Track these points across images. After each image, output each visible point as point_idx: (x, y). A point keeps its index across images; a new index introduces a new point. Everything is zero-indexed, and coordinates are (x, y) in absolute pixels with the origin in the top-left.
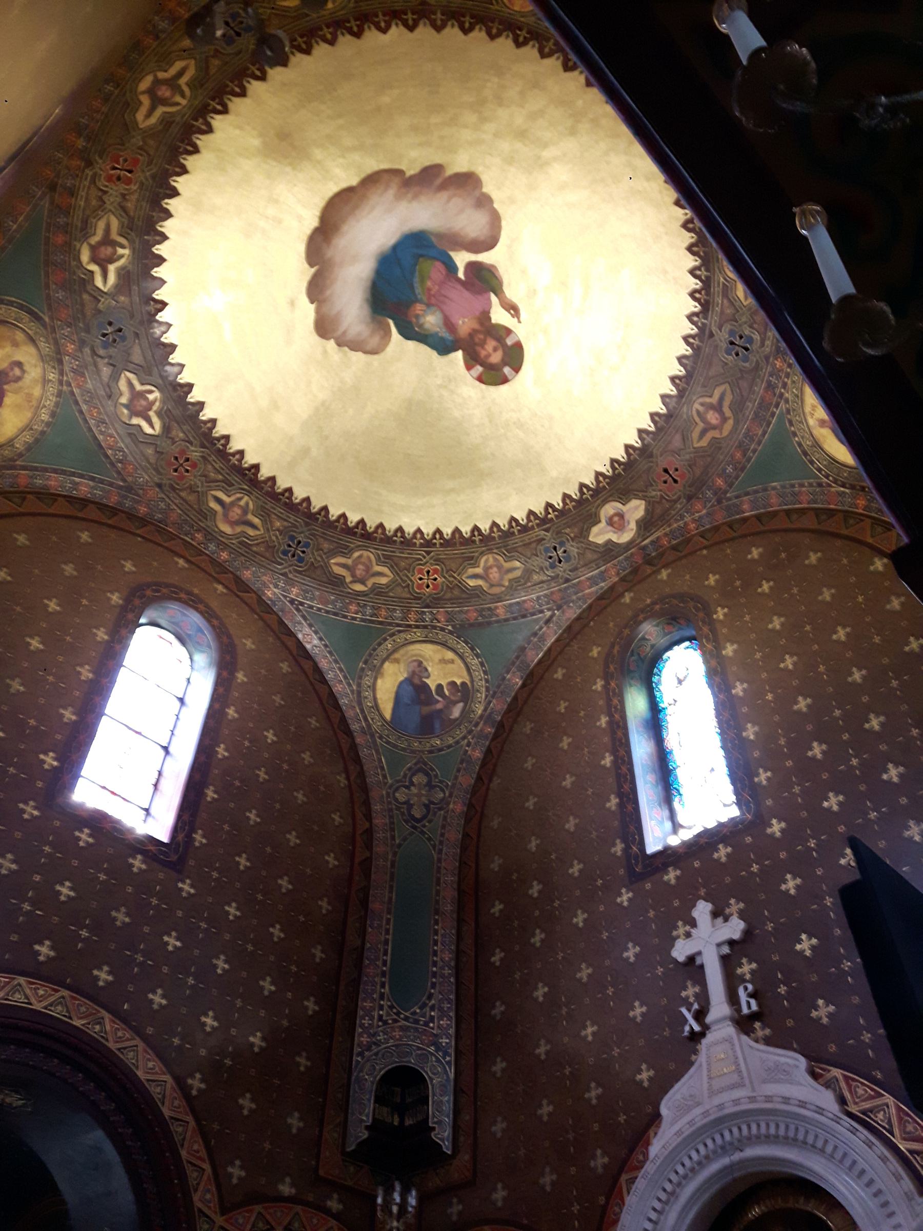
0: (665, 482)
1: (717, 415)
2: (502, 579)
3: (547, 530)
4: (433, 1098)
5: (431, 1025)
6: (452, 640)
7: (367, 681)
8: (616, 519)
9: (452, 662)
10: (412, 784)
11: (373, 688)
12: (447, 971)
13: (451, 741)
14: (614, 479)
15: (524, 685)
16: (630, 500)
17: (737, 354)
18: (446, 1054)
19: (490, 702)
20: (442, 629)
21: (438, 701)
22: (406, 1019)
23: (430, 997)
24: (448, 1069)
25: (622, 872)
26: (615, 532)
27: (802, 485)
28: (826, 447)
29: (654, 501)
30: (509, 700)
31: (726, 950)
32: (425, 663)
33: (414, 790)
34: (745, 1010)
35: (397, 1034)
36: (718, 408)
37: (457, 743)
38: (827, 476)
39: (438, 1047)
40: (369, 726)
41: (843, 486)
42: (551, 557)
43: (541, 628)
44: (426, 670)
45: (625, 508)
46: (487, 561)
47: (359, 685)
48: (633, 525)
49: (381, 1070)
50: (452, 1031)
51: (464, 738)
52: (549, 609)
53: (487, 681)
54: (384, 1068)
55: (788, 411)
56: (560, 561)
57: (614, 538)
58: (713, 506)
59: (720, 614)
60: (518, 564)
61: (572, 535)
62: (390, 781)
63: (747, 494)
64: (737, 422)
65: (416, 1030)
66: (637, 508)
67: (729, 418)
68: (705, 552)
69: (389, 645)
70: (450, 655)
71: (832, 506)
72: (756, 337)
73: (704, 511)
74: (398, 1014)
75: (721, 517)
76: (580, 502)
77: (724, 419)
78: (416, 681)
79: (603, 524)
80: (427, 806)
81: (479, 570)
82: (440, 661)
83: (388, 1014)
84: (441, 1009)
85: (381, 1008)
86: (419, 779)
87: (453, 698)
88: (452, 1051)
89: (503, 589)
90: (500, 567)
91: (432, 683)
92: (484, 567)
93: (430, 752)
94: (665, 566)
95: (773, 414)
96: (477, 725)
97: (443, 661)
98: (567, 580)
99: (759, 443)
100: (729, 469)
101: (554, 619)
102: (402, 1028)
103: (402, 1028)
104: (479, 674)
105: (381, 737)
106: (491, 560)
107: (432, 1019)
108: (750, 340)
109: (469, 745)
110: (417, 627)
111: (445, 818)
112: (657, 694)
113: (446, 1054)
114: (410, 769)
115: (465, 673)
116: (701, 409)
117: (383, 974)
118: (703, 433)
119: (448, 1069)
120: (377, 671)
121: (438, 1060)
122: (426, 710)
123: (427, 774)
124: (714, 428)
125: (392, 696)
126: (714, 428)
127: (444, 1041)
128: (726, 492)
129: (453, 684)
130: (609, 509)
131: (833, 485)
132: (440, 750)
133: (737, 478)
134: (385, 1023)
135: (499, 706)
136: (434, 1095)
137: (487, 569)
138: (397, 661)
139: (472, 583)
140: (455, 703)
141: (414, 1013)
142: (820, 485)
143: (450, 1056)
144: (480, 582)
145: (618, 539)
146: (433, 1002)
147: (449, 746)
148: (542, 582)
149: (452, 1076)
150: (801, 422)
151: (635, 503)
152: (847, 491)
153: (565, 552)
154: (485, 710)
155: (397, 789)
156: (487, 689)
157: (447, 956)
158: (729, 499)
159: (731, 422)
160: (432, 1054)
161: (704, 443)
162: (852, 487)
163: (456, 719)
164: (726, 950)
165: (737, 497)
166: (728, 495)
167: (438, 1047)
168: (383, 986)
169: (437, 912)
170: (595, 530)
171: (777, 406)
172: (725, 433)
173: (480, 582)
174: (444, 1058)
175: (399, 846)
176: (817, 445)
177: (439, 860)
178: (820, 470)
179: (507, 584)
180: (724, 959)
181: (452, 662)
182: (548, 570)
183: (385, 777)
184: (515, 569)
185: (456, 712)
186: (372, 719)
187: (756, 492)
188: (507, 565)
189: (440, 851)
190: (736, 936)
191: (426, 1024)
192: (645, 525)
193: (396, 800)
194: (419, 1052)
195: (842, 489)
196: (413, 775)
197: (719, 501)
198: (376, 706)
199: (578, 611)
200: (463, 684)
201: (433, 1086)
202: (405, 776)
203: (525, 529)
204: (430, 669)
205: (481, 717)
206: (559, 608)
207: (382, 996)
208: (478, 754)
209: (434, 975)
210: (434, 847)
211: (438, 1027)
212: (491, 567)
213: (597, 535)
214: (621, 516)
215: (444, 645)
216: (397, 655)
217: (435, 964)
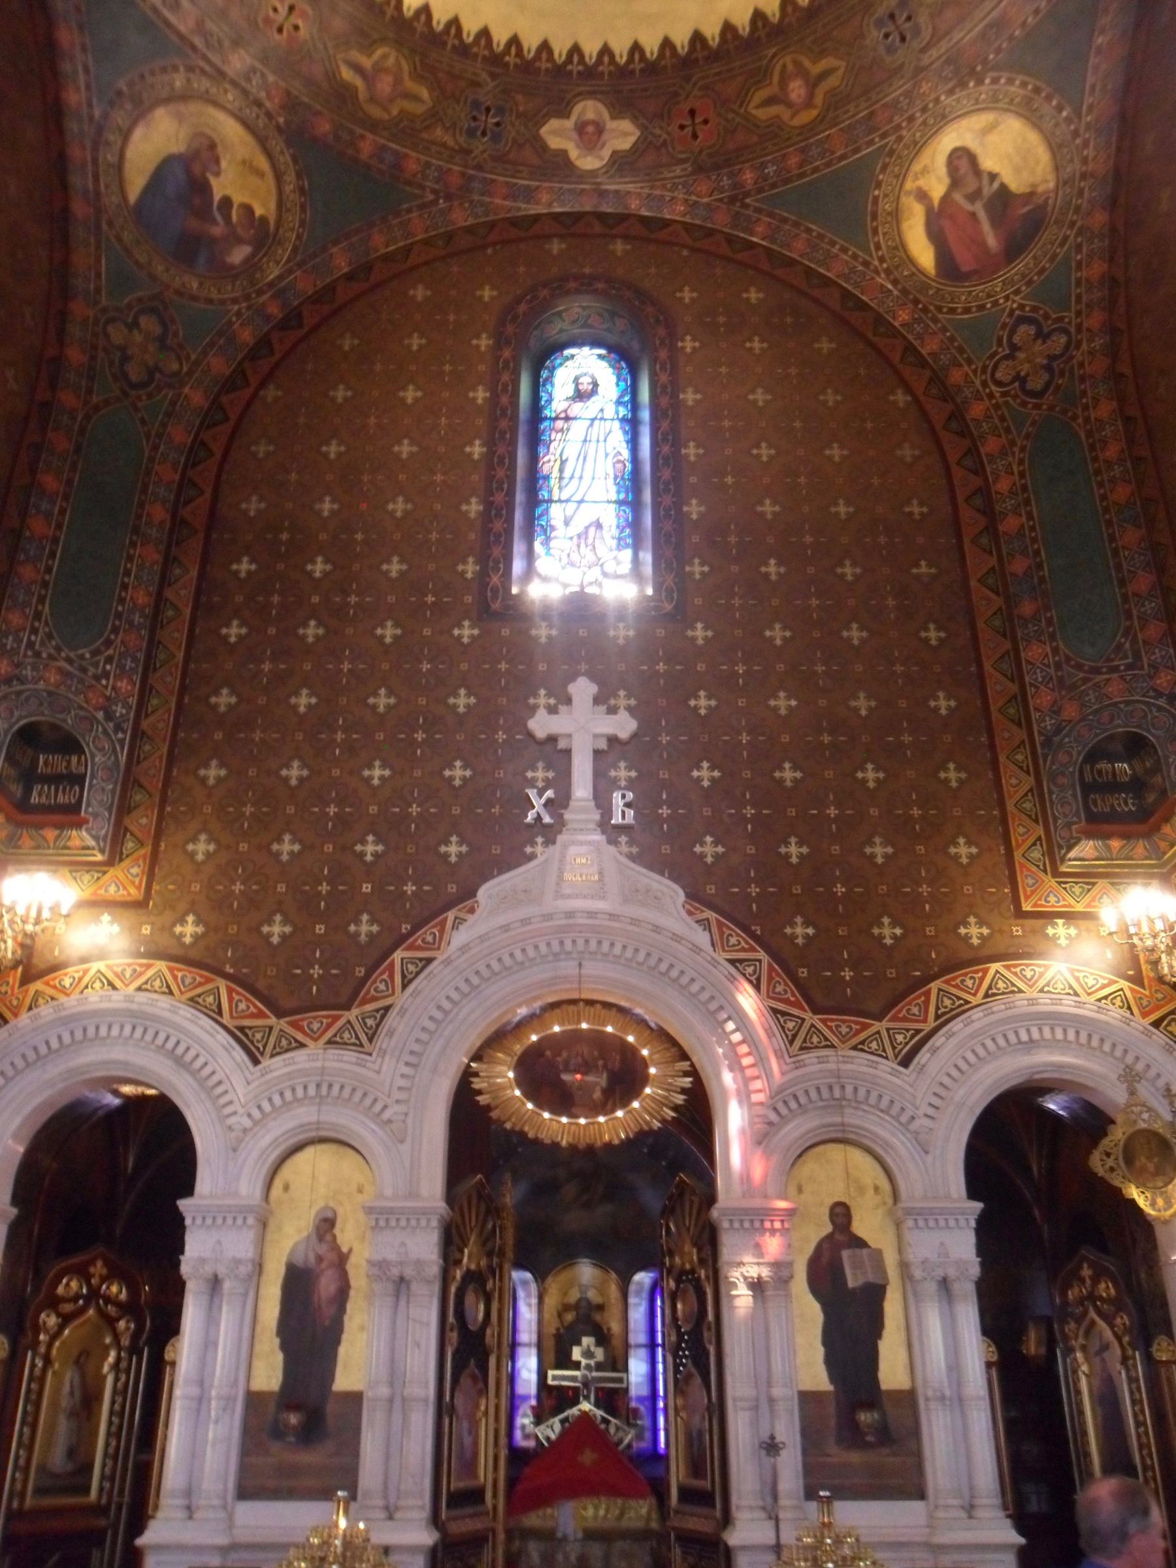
0: (682, 127)
1: (803, 92)
2: (392, 100)
3: (493, 76)
4: (91, 780)
5: (104, 682)
6: (277, 144)
7: (120, 118)
8: (590, 129)
9: (261, 174)
10: (135, 324)
11: (126, 136)
12: (137, 619)
13: (214, 295)
14: (623, 72)
15: (350, 277)
16: (622, 118)
17: (887, 36)
18: (118, 728)
19: (290, 272)
20: (269, 115)
21: (215, 222)
22: (69, 660)
23: (108, 643)
24: (118, 748)
25: (468, 599)
26: (578, 147)
27: (844, 250)
28: (905, 226)
29: (651, 143)
30: (320, 284)
31: (603, 745)
32: (220, 149)
33: (138, 337)
34: (617, 819)
35: (53, 677)
36: (813, 84)
37: (222, 302)
38: (882, 260)
39: (109, 716)
40: (97, 193)
41: (895, 282)
42: (475, 119)
43: (409, 211)
44: (217, 161)
45: (611, 125)
46: (384, 57)
47: (105, 116)
48: (606, 153)
49: (20, 718)
50: (133, 701)
51: (235, 301)
52: (434, 191)
53: (299, 237)
54: (26, 717)
55: (891, 153)
56: (484, 134)
57: (573, 153)
58: (721, 200)
59: (688, 344)
60: (425, 94)
61: (521, 109)
62: (104, 302)
63: (771, 215)
64: (821, 119)
65: (81, 681)
66: (626, 134)
67: (815, 107)
68: (685, 253)
69: (179, 82)
70: (263, 163)
71: (864, 298)
72: (926, 35)
73: (705, 200)
74: (58, 649)
75: (721, 221)
76: (560, 71)
77: (809, 103)
78: (197, 169)
79: (569, 124)
80: (152, 371)
81: (367, 62)
82: (244, 162)
83: (42, 643)
84: (121, 667)
85: (35, 631)
86: (148, 323)
87: (239, 230)
88: (129, 726)
89: (386, 117)
90: (398, 81)
91: (221, 187)
92: (377, 63)
93: (178, 293)
94: (626, 238)
95: (871, 143)
96: (260, 293)
97: (248, 166)
98: (479, 167)
99: (828, 165)
100: (771, 170)
101: (434, 209)
102: (60, 671)
103: (60, 671)
104: (293, 219)
105: (110, 224)
106: (391, 61)
107: (106, 675)
108: (917, 32)
109: (239, 314)
110: (234, 83)
111: (173, 403)
112: (544, 397)
113: (118, 728)
114: (140, 300)
115: (273, 206)
116: (790, 67)
117: (45, 584)
118: (770, 101)
119: (118, 748)
120: (141, 111)
121: (105, 731)
122: (194, 224)
123: (163, 324)
124: (789, 105)
125: (150, 168)
126: (789, 105)
127: (119, 710)
128: (747, 194)
129: (248, 210)
130: (589, 109)
131: (883, 275)
132: (194, 298)
133: (773, 186)
134: (37, 655)
135: (306, 285)
136: (93, 777)
137: (379, 69)
138: (180, 118)
139: (347, 74)
140: (240, 241)
141: (82, 657)
142: (866, 264)
143: (124, 732)
144: (359, 82)
145: (578, 157)
146: (110, 652)
147: (210, 301)
148: (444, 145)
149: (123, 759)
150: (897, 176)
151: (626, 125)
152: (896, 293)
153: (498, 124)
154: (280, 277)
155: (112, 320)
156: (295, 250)
157: (142, 599)
158: (745, 206)
159: (814, 113)
160: (98, 722)
161: (762, 114)
162: (905, 292)
163: (233, 267)
164: (603, 745)
165: (758, 210)
166: (748, 201)
167: (109, 716)
168: (41, 599)
169: (136, 530)
170: (554, 124)
171: (883, 136)
172: (796, 122)
173: (359, 82)
174: (116, 733)
175: (97, 408)
176: (896, 216)
177: (152, 459)
178: (878, 247)
179: (395, 112)
180: (597, 753)
181: (261, 174)
182: (461, 135)
183: (98, 290)
184: (416, 98)
185: (238, 255)
186: (107, 186)
187: (785, 220)
188: (410, 85)
189: (155, 448)
190: (624, 735)
191: (97, 678)
192: (621, 163)
193: (107, 336)
194: (82, 713)
195: (890, 286)
196: (142, 311)
197: (732, 200)
198: (119, 167)
199: (471, 221)
200: (264, 220)
201: (93, 764)
202: (129, 306)
203: (463, 50)
204: (224, 164)
205: (271, 285)
206: (449, 197)
207: (38, 615)
208: (247, 336)
209: (119, 616)
210: (148, 436)
211: (114, 688)
212: (386, 70)
213: (554, 133)
214: (600, 129)
215: (262, 141)
216: (182, 107)
217: (122, 601)
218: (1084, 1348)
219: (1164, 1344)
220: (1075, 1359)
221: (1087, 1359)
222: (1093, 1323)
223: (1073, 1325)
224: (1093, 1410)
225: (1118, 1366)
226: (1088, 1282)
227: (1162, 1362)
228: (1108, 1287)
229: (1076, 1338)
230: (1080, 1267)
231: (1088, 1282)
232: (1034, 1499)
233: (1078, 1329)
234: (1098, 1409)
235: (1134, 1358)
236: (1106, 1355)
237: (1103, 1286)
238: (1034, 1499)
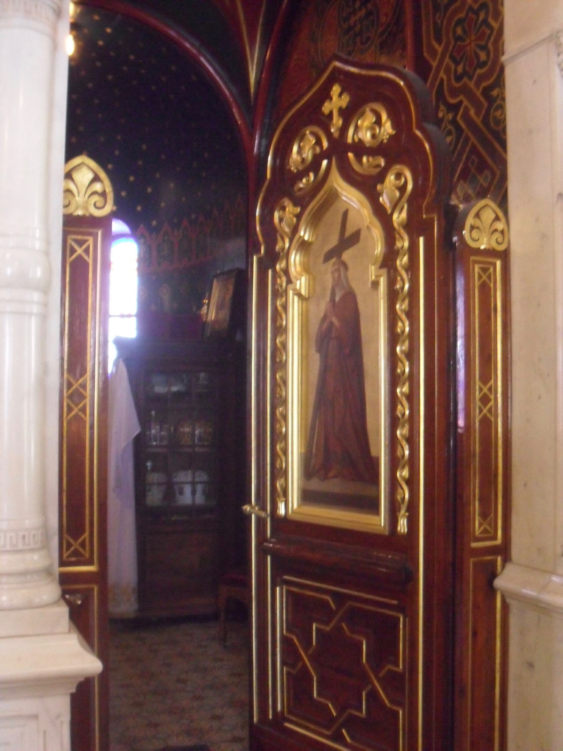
218: (304, 246)
219: (488, 215)
220: (286, 272)
221: (307, 269)
222: (334, 196)
223: (291, 209)
224: (305, 359)
225: (373, 270)
226: (337, 121)
227: (478, 252)
228: (378, 122)
229: (295, 230)
230: (325, 95)
231: (337, 121)
232: (188, 489)
233: (299, 217)
234: (316, 359)
235: (413, 250)
236: (347, 256)
237: (368, 120)
238: (188, 489)
